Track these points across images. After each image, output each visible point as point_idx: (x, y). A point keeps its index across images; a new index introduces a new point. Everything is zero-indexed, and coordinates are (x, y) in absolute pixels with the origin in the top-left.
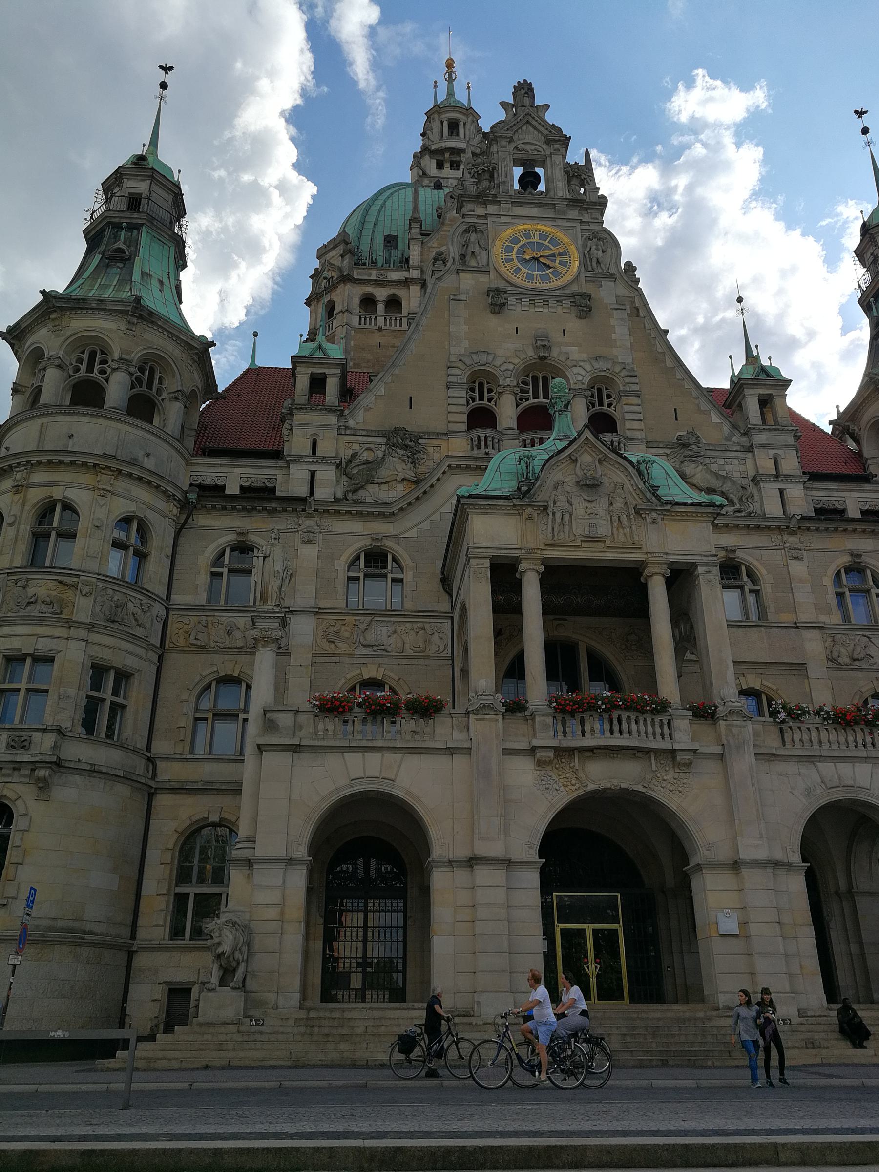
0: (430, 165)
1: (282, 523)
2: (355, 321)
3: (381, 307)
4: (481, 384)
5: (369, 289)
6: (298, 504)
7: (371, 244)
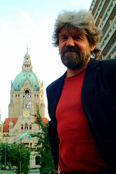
0: (24, 66)
1: (9, 137)
2: (15, 98)
4: (22, 125)
5: (16, 94)
6: (9, 136)
7: (17, 87)
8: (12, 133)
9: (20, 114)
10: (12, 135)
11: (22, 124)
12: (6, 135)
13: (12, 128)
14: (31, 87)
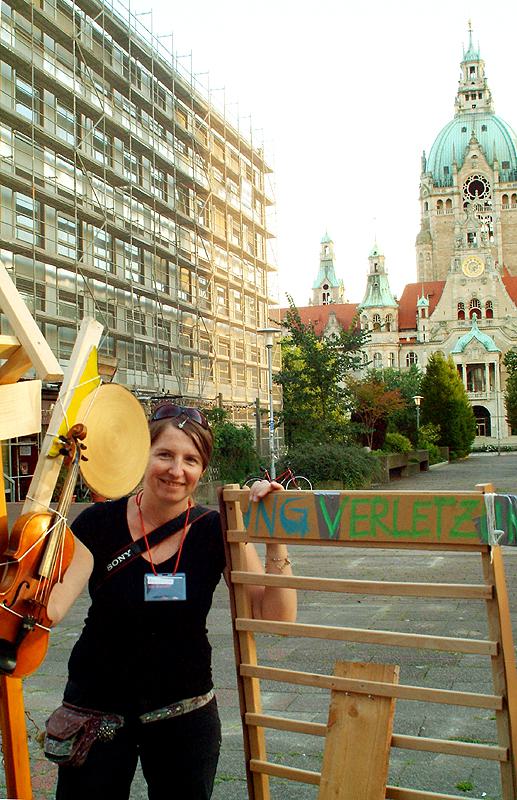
0: (463, 97)
1: (419, 347)
3: (445, 205)
4: (461, 305)
5: (440, 198)
7: (439, 175)
8: (427, 334)
9: (452, 267)
10: (427, 340)
11: (461, 301)
12: (408, 340)
13: (427, 315)
14: (488, 169)
